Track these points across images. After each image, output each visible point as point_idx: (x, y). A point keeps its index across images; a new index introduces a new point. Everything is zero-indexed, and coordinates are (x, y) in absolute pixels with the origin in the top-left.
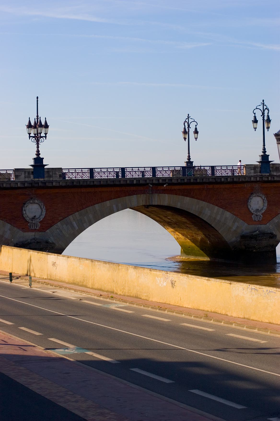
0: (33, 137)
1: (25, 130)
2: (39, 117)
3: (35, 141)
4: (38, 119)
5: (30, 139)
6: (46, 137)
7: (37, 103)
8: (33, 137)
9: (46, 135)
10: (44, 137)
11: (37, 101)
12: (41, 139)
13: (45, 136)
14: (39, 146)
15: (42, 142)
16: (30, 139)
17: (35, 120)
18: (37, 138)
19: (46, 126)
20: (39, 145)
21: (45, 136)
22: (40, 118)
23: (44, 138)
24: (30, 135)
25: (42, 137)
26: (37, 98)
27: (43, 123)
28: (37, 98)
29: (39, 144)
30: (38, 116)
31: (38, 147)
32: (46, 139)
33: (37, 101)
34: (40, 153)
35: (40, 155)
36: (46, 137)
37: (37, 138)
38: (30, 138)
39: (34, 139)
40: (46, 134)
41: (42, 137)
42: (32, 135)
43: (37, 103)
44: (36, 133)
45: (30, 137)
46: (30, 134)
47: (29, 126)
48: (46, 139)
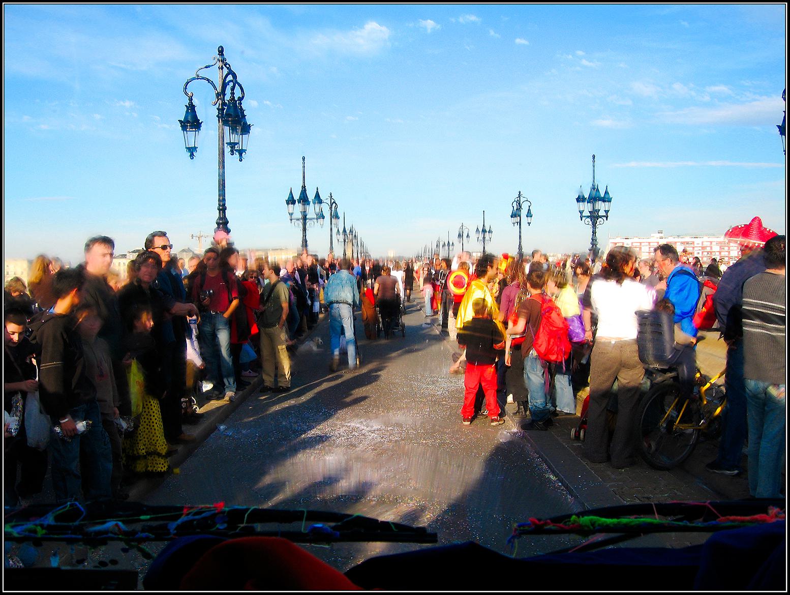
0: (588, 217)
5: (581, 220)
8: (588, 217)
10: (604, 216)
12: (600, 219)
16: (581, 220)
18: (594, 217)
19: (606, 199)
22: (598, 185)
23: (605, 218)
25: (601, 217)
31: (594, 233)
32: (607, 220)
37: (594, 217)
40: (607, 212)
41: (601, 217)
42: (586, 213)
46: (581, 212)
48: (607, 220)
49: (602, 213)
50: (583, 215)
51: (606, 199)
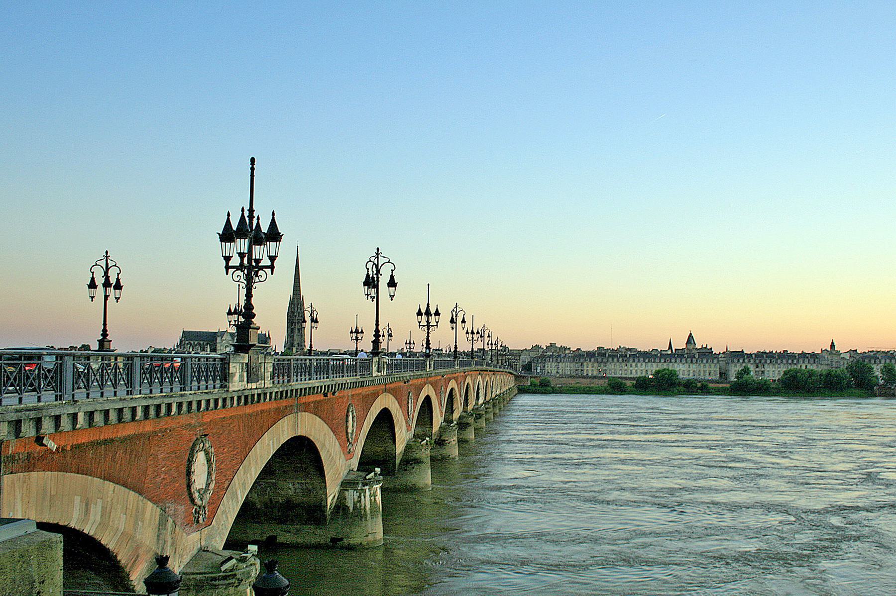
1: (216, 248)
2: (255, 215)
3: (242, 280)
4: (251, 217)
5: (227, 274)
6: (274, 267)
7: (252, 176)
8: (237, 268)
9: (272, 262)
10: (267, 267)
11: (252, 169)
12: (261, 273)
13: (269, 264)
14: (254, 292)
15: (260, 281)
16: (227, 274)
17: (243, 215)
19: (274, 235)
20: (253, 290)
21: (269, 264)
22: (258, 218)
23: (268, 271)
24: (227, 263)
25: (262, 268)
26: (253, 161)
27: (265, 229)
28: (253, 161)
29: (254, 286)
30: (251, 211)
32: (272, 273)
33: (252, 169)
34: (254, 311)
35: (253, 318)
36: (272, 267)
38: (230, 270)
39: (239, 272)
40: (272, 259)
41: (262, 268)
42: (235, 261)
43: (252, 176)
44: (246, 251)
45: (227, 268)
46: (227, 259)
47: (227, 236)
48: (272, 273)
49: (266, 262)
50: (230, 264)
51: (274, 235)
